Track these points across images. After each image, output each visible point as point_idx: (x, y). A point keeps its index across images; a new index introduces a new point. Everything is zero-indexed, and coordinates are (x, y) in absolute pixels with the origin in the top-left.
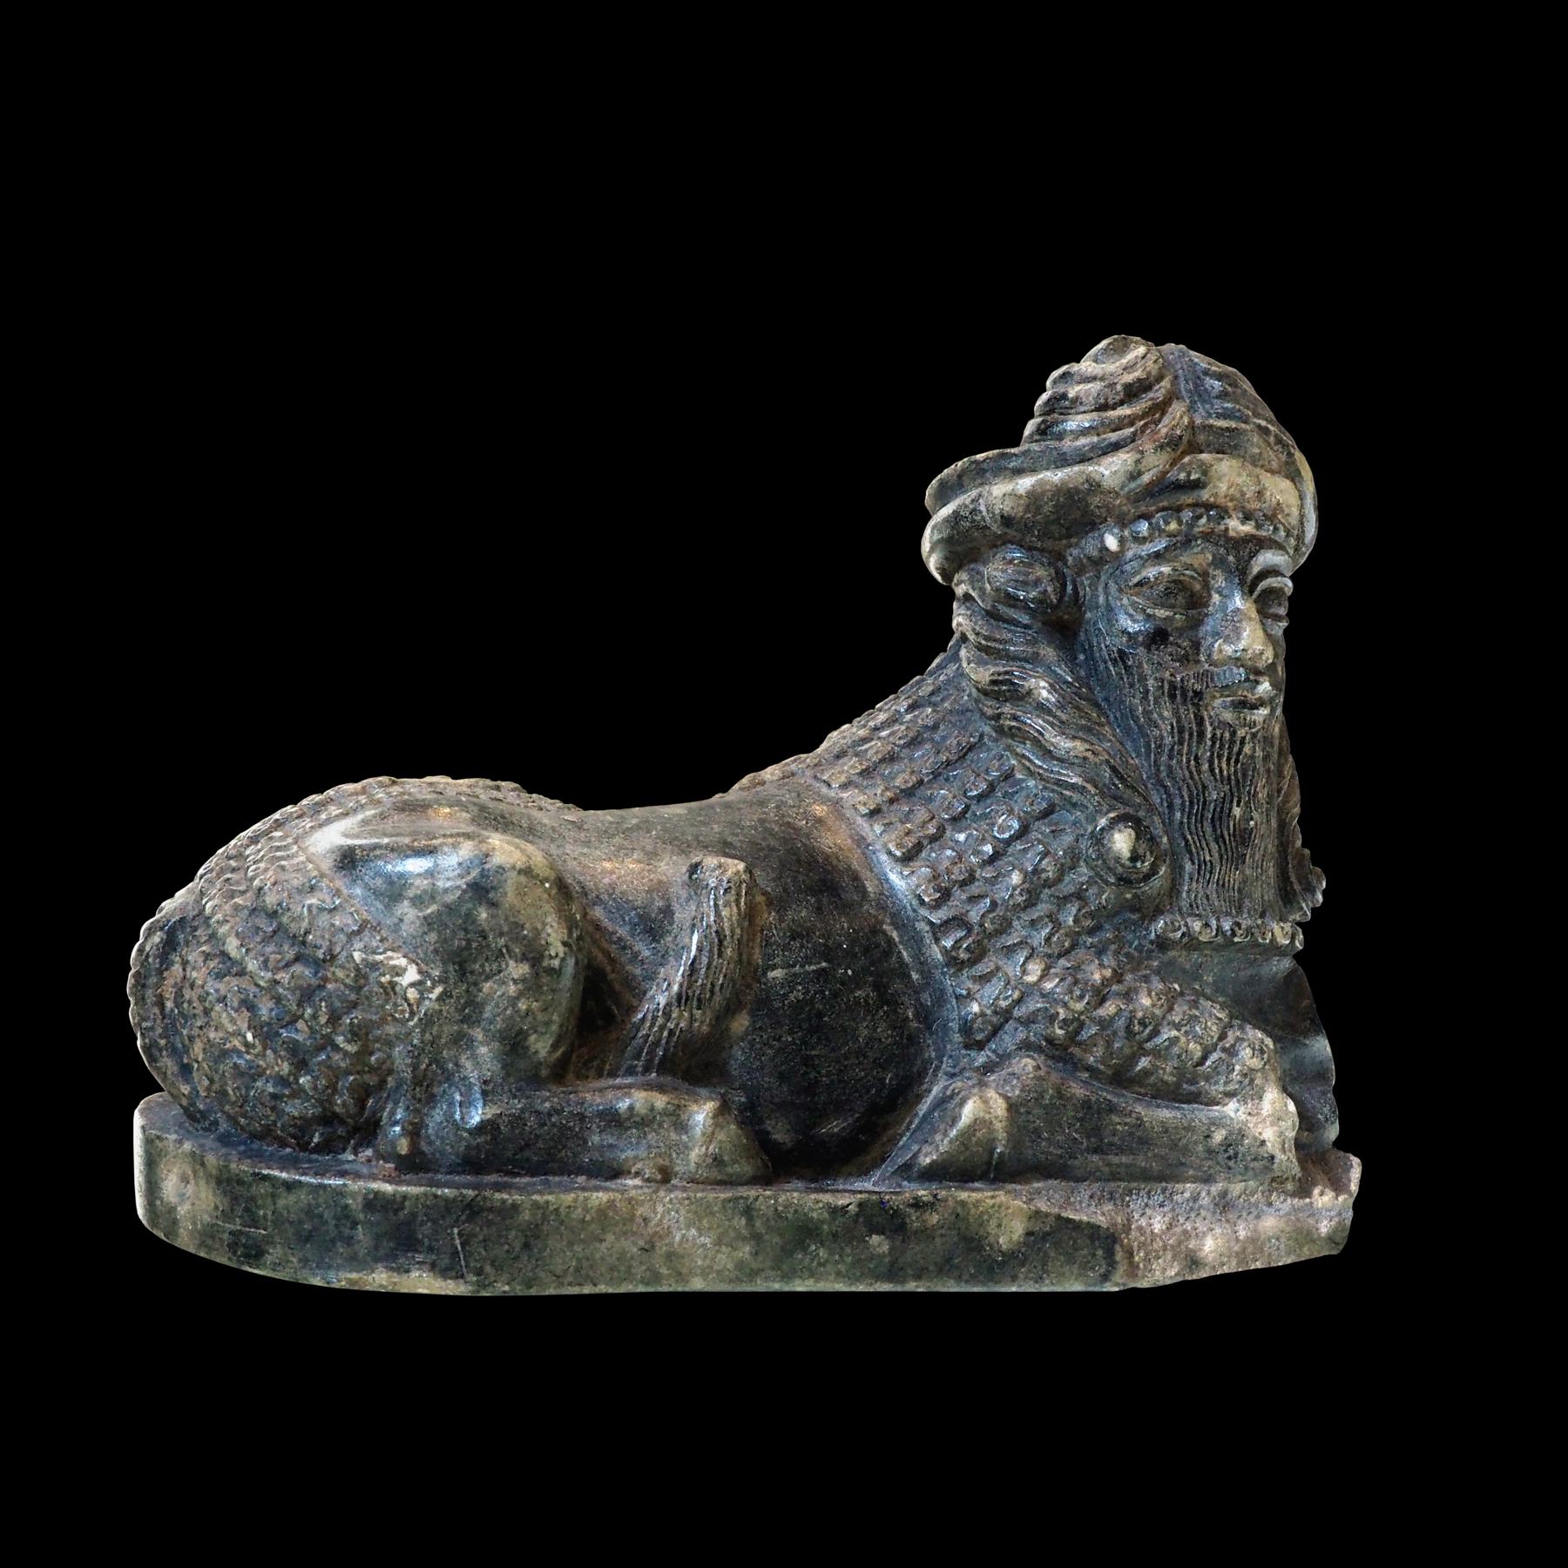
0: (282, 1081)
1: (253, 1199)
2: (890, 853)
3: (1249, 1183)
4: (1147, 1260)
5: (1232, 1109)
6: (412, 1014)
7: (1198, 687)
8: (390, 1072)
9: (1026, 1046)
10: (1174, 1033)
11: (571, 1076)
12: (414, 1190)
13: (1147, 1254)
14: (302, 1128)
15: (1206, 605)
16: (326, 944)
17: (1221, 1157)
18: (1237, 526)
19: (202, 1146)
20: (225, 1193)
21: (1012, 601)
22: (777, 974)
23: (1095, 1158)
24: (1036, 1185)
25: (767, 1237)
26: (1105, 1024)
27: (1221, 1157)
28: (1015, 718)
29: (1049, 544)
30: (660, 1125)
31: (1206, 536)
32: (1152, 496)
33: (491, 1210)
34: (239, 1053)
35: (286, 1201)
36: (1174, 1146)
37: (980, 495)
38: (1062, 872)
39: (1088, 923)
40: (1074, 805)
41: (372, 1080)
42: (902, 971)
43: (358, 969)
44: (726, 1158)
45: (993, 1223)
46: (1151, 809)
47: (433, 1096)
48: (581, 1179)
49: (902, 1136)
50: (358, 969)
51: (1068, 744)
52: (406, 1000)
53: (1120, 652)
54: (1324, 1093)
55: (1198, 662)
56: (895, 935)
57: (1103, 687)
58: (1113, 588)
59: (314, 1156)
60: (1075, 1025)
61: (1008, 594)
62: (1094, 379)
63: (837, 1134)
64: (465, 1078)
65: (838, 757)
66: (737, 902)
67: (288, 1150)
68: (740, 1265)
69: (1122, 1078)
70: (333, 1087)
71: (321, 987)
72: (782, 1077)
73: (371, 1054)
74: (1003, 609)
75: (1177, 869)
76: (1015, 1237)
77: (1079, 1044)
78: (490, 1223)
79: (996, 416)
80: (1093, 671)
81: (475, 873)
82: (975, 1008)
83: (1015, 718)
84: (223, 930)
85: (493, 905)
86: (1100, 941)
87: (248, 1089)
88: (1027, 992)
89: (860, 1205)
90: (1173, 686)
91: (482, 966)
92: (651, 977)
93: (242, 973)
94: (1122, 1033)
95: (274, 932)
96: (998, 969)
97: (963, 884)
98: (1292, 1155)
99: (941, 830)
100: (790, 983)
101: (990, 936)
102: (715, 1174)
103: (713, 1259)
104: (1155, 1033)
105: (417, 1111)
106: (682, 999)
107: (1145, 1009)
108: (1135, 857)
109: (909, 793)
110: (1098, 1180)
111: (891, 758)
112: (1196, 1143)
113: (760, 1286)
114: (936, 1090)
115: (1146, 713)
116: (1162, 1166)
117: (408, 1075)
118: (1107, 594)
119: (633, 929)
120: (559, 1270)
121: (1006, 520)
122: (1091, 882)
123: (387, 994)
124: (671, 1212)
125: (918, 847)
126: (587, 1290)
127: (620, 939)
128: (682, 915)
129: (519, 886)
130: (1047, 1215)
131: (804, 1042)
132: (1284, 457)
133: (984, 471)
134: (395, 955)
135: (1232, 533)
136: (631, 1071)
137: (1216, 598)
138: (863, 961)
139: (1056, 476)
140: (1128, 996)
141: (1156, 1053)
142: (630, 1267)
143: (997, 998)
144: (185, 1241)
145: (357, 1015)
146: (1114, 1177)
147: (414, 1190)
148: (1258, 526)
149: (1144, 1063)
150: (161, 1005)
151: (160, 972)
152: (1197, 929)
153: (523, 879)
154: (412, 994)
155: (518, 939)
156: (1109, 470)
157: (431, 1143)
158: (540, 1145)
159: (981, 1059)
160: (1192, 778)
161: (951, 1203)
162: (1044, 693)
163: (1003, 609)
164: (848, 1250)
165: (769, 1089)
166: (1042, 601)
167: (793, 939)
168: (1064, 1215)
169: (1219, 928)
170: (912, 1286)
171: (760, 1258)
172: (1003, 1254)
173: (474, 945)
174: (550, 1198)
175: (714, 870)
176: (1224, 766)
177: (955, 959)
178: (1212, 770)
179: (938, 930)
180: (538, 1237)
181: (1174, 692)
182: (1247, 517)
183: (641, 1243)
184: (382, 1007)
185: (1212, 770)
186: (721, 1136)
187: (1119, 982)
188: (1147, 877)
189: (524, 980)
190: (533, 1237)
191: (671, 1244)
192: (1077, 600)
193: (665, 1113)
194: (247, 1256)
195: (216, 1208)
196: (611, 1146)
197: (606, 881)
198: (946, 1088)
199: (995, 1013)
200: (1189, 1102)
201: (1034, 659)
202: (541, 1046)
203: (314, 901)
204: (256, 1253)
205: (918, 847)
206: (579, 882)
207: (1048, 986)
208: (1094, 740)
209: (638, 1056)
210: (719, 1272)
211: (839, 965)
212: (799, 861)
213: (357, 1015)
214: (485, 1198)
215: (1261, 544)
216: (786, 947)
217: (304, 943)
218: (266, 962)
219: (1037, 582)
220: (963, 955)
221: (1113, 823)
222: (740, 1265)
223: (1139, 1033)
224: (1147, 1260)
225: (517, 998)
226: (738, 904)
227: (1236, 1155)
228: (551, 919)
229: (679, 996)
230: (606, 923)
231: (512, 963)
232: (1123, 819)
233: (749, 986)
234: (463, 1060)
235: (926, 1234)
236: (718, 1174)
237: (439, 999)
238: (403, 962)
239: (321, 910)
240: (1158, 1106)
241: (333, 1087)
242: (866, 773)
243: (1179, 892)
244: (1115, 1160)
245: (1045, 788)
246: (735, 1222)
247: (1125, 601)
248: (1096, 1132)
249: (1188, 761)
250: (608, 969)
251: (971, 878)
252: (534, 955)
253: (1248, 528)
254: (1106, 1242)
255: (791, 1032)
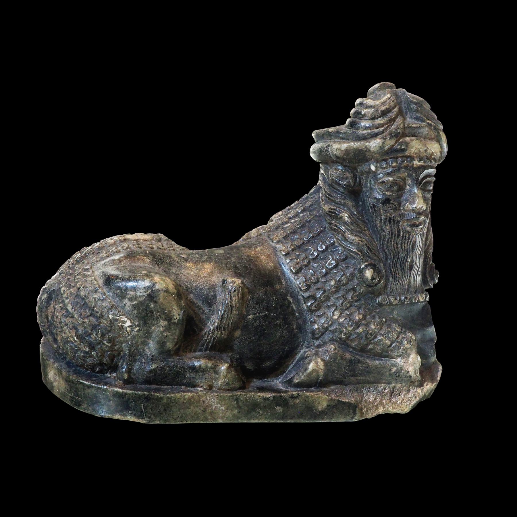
0: (87, 353)
1: (77, 388)
2: (291, 270)
3: (405, 381)
4: (367, 411)
5: (399, 361)
6: (129, 335)
7: (399, 219)
8: (122, 351)
9: (332, 340)
10: (382, 337)
11: (181, 352)
12: (129, 392)
13: (367, 409)
14: (93, 368)
15: (404, 189)
16: (100, 312)
17: (394, 377)
18: (417, 163)
19: (61, 366)
20: (68, 385)
21: (338, 184)
22: (251, 317)
23: (352, 378)
24: (332, 387)
25: (243, 407)
26: (358, 334)
27: (394, 377)
28: (336, 226)
29: (352, 165)
30: (209, 372)
31: (406, 167)
32: (388, 154)
33: (153, 399)
34: (72, 342)
35: (87, 391)
36: (379, 373)
37: (329, 145)
38: (348, 281)
39: (355, 298)
40: (354, 258)
41: (116, 353)
42: (293, 313)
43: (111, 321)
44: (230, 383)
45: (317, 403)
46: (380, 260)
47: (135, 359)
48: (183, 387)
49: (290, 365)
50: (111, 321)
51: (354, 238)
52: (127, 331)
53: (373, 204)
54: (432, 346)
55: (400, 210)
56: (291, 300)
57: (367, 215)
58: (373, 182)
59: (97, 374)
60: (349, 335)
61: (336, 182)
62: (370, 107)
63: (269, 366)
64: (146, 354)
65: (277, 229)
66: (238, 295)
67: (89, 371)
68: (234, 416)
69: (363, 350)
70: (103, 355)
71: (99, 325)
72: (251, 350)
73: (115, 346)
74: (335, 185)
75: (387, 279)
76: (324, 407)
77: (350, 340)
78: (153, 403)
79: (337, 112)
80: (364, 209)
81: (149, 291)
82: (316, 326)
83: (336, 226)
84: (67, 301)
85: (155, 302)
86: (359, 304)
87: (75, 353)
88: (334, 322)
89: (274, 397)
90: (390, 219)
91: (152, 322)
92: (209, 318)
93: (73, 317)
94: (364, 338)
95: (84, 304)
96: (324, 313)
97: (315, 283)
98: (418, 374)
99: (309, 262)
100: (255, 320)
101: (323, 302)
102: (227, 387)
103: (225, 414)
104: (376, 337)
105: (130, 364)
106: (218, 328)
107: (372, 330)
108: (373, 279)
109: (299, 247)
110: (353, 384)
111: (294, 232)
112: (386, 372)
113: (240, 421)
114: (302, 351)
115: (381, 227)
116: (374, 378)
117: (127, 352)
118: (370, 183)
119: (203, 303)
120: (175, 417)
121: (337, 157)
122: (358, 285)
123: (120, 329)
124: (212, 398)
125: (301, 269)
126: (184, 423)
127: (199, 306)
128: (220, 297)
129: (164, 296)
130: (335, 400)
131: (259, 339)
132: (436, 134)
133: (331, 136)
134: (123, 317)
135: (415, 166)
136: (201, 350)
137: (408, 187)
138: (279, 310)
139: (354, 145)
140: (367, 325)
141: (376, 343)
142: (198, 416)
143: (324, 323)
144: (56, 392)
145: (111, 335)
146: (358, 383)
147: (129, 392)
148: (424, 162)
149: (371, 346)
150: (47, 318)
151: (47, 307)
152: (392, 301)
153: (165, 294)
154: (128, 329)
155: (163, 313)
156: (374, 144)
157: (135, 375)
158: (170, 377)
159: (317, 343)
160: (395, 249)
161: (303, 396)
162: (346, 219)
163: (335, 185)
164: (269, 411)
165: (246, 354)
166: (347, 185)
167: (257, 304)
168: (340, 400)
169: (400, 299)
170: (289, 421)
171: (240, 414)
172: (320, 412)
173: (149, 315)
174: (173, 395)
175: (230, 283)
176: (406, 245)
177: (311, 310)
178: (401, 247)
179: (306, 300)
180: (168, 407)
181: (391, 220)
182: (420, 160)
183: (202, 409)
184: (119, 333)
185: (401, 247)
186: (229, 376)
187: (365, 319)
188: (376, 285)
189: (165, 326)
190: (167, 408)
191: (212, 409)
192: (360, 185)
193: (211, 368)
194: (76, 405)
195: (66, 388)
196: (193, 378)
197: (195, 284)
198: (305, 352)
199: (323, 328)
200: (385, 358)
201: (344, 205)
202: (169, 345)
203: (96, 296)
204: (79, 404)
205: (301, 269)
206: (186, 285)
207: (341, 320)
208: (362, 236)
209: (203, 346)
210: (227, 418)
211: (272, 313)
212: (260, 274)
213: (111, 335)
214: (151, 395)
215: (424, 168)
216: (254, 307)
217: (93, 310)
218: (81, 315)
219: (347, 178)
220: (313, 308)
221: (366, 266)
222: (234, 416)
223: (370, 337)
224: (367, 411)
225: (163, 332)
226: (238, 296)
227: (399, 376)
228: (175, 307)
229: (217, 327)
230: (194, 300)
231: (161, 321)
232: (369, 265)
233: (241, 321)
234: (145, 348)
235: (295, 406)
236: (228, 388)
237: (137, 331)
238: (126, 319)
239: (99, 300)
240: (375, 360)
241: (103, 355)
242: (285, 238)
243: (387, 288)
244: (359, 378)
245: (344, 251)
246: (233, 403)
247: (376, 187)
248: (353, 370)
249: (394, 244)
250: (194, 316)
251: (318, 281)
252: (169, 318)
253: (422, 163)
254: (353, 408)
255: (254, 336)
